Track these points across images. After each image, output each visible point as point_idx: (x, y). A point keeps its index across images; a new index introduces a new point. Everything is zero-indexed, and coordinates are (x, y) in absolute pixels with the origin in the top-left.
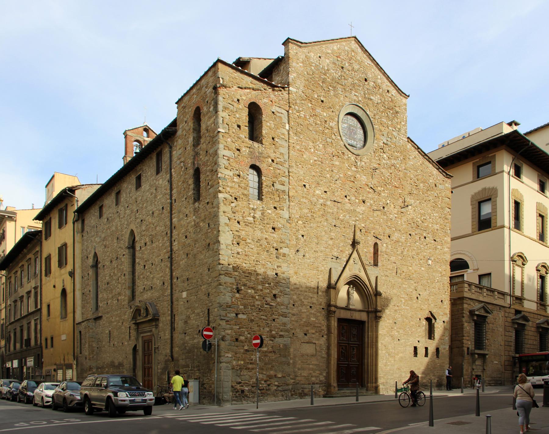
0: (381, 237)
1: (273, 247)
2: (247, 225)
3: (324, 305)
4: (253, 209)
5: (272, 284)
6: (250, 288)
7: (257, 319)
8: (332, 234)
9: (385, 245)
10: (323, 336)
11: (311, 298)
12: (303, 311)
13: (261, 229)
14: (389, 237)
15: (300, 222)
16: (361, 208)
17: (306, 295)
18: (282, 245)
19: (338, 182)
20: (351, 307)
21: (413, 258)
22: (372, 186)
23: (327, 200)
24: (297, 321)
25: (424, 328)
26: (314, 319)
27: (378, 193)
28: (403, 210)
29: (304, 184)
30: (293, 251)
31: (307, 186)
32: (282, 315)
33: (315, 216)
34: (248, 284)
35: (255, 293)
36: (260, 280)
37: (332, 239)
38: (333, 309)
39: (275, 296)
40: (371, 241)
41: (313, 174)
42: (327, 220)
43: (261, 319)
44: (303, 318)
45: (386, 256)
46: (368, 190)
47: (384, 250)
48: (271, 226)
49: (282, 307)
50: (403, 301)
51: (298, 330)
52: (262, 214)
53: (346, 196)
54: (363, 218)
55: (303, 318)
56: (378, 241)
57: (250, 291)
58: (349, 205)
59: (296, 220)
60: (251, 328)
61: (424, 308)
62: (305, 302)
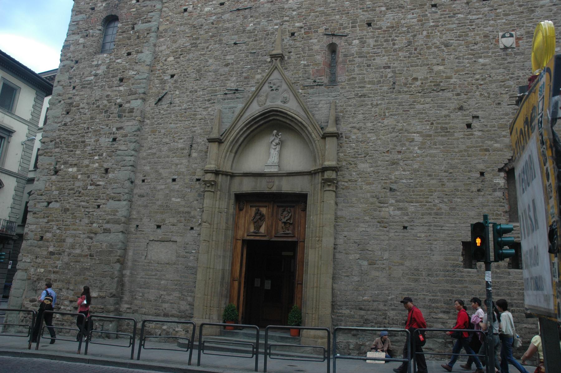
0: (347, 31)
5: (104, 154)
6: (71, 165)
7: (74, 207)
9: (356, 42)
10: (192, 228)
11: (177, 165)
12: (159, 188)
15: (172, 58)
17: (167, 162)
18: (130, 97)
23: (223, 13)
24: (146, 206)
25: (499, 194)
26: (179, 200)
29: (185, 7)
30: (152, 101)
31: (190, 8)
32: (113, 198)
36: (88, 152)
37: (227, 65)
38: (210, 177)
39: (107, 170)
40: (318, 43)
43: (79, 206)
49: (115, 186)
50: (418, 138)
51: (145, 220)
52: (108, 68)
54: (299, 15)
55: (158, 200)
56: (335, 40)
57: (70, 170)
59: (164, 58)
61: (497, 145)
62: (164, 173)
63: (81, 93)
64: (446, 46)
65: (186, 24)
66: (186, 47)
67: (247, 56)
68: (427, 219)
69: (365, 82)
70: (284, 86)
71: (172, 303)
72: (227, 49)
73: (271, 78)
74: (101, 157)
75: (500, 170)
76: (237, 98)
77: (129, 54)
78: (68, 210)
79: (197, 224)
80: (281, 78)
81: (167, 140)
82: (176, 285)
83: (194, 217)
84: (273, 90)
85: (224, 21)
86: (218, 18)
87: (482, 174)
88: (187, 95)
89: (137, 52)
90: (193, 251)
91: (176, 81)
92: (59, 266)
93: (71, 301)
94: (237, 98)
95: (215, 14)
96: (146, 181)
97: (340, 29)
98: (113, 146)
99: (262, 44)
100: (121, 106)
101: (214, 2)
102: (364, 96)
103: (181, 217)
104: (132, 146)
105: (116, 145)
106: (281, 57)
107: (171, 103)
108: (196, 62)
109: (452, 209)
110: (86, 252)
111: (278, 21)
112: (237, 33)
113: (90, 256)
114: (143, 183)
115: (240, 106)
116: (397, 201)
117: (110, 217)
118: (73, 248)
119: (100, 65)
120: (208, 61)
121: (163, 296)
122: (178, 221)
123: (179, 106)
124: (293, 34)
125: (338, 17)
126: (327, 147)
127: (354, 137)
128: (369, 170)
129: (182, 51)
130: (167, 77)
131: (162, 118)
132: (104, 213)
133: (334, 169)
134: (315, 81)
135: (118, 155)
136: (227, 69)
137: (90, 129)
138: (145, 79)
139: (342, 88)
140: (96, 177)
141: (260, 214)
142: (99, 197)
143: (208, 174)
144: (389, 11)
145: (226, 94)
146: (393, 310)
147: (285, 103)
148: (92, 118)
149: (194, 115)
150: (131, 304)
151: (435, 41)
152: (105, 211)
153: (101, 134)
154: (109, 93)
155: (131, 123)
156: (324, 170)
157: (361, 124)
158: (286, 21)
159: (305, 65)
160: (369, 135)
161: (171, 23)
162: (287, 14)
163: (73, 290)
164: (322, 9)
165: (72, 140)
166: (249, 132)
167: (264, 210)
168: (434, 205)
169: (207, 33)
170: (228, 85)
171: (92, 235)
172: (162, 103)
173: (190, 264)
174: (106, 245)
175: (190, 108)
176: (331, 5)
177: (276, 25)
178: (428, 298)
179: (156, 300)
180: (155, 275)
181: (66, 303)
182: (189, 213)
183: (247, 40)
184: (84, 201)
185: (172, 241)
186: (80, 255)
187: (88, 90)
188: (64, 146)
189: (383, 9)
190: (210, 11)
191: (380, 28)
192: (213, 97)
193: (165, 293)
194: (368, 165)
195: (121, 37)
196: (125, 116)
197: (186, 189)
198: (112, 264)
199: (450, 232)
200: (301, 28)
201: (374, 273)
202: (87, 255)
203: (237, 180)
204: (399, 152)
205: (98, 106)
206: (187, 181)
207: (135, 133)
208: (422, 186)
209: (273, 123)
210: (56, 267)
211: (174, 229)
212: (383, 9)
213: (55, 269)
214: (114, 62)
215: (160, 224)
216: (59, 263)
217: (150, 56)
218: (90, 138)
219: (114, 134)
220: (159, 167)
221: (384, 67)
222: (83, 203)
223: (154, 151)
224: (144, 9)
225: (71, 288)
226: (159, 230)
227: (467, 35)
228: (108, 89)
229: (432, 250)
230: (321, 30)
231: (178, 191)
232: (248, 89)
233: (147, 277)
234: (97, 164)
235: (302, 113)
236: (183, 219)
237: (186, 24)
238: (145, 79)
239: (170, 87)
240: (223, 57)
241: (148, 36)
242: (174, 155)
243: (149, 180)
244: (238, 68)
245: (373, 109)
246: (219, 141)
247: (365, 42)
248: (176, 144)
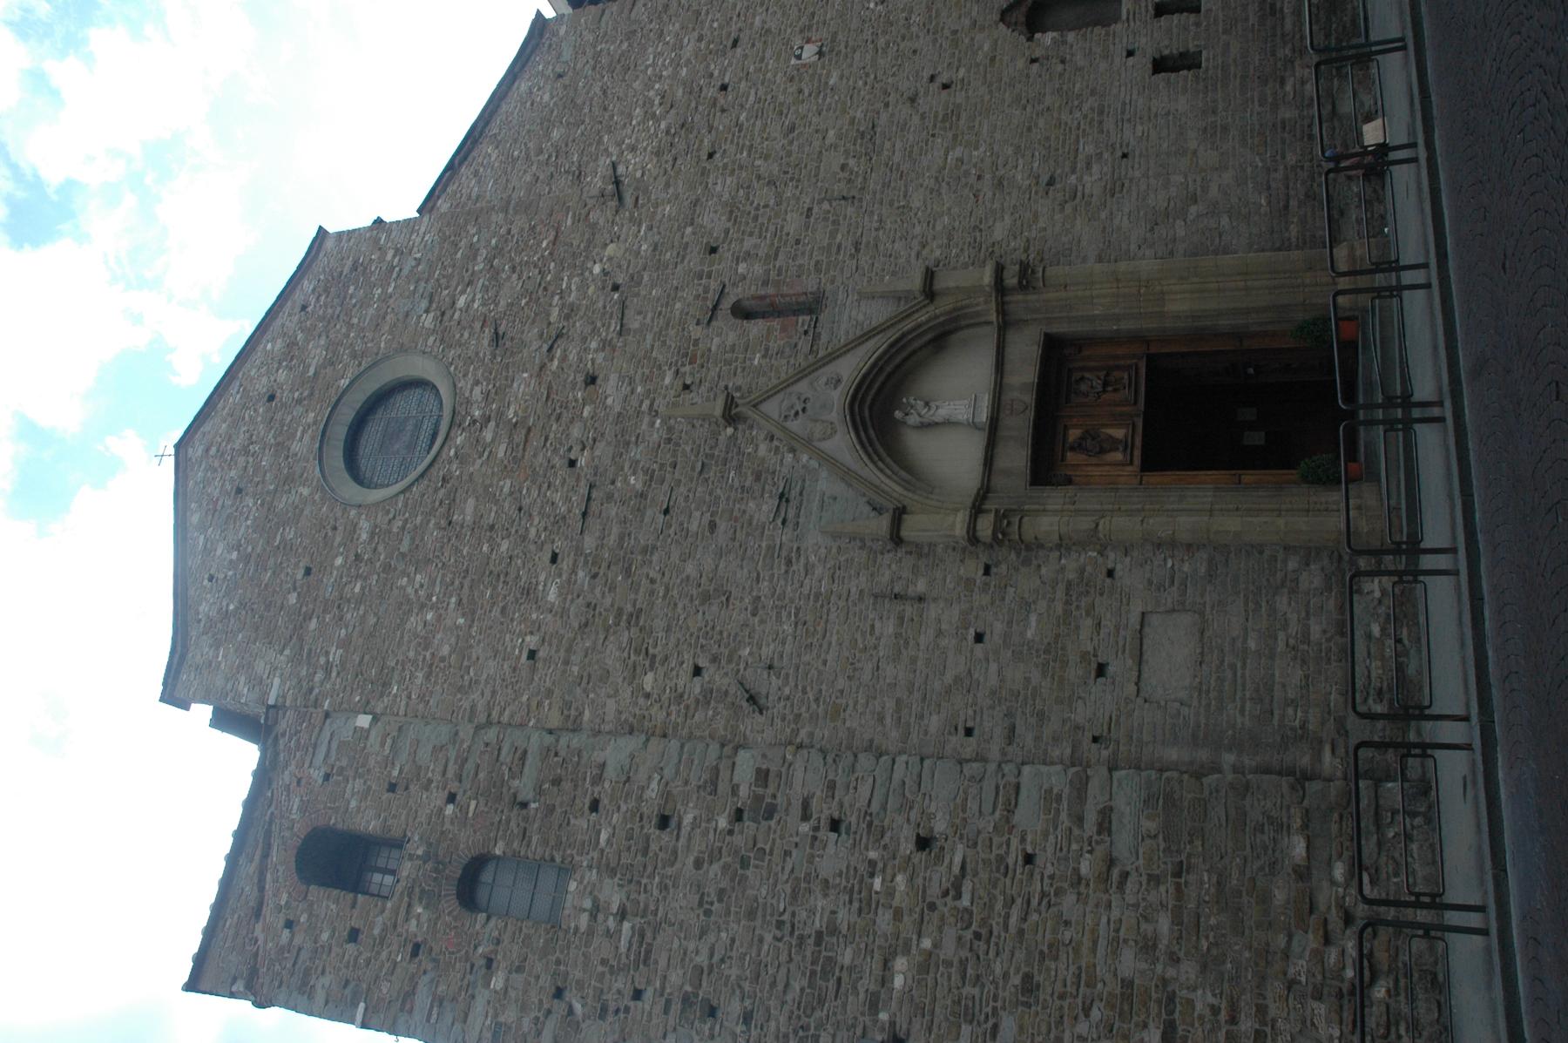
0: (714, 285)
1: (731, 832)
2: (648, 952)
3: (973, 569)
4: (593, 917)
5: (873, 855)
6: (885, 981)
7: (1020, 955)
8: (694, 527)
9: (742, 268)
10: (1110, 573)
11: (940, 633)
12: (993, 680)
13: (664, 888)
14: (713, 250)
15: (648, 681)
16: (612, 392)
18: (723, 787)
19: (526, 502)
20: (983, 417)
21: (792, 129)
22: (545, 347)
23: (579, 550)
24: (1041, 716)
25: (1071, 37)
26: (1033, 618)
27: (567, 317)
28: (629, 200)
29: (525, 655)
30: (752, 724)
31: (532, 641)
32: (1010, 810)
33: (629, 608)
34: (867, 984)
35: (907, 951)
36: (854, 918)
37: (713, 526)
38: (985, 526)
39: (923, 843)
40: (728, 332)
41: (496, 612)
42: (645, 551)
43: (1021, 932)
44: (1027, 680)
45: (781, 257)
46: (556, 362)
47: (758, 269)
48: (653, 832)
49: (973, 805)
50: (958, 152)
51: (1080, 714)
52: (613, 873)
53: (572, 463)
54: (646, 379)
55: (1027, 680)
56: (726, 304)
57: (898, 981)
58: (601, 445)
59: (641, 701)
60: (1062, 997)
61: (986, 47)
63: (662, 963)
64: (792, 129)
65: (569, 650)
66: (631, 640)
67: (706, 480)
68: (1109, 124)
69: (830, 245)
70: (802, 387)
71: (1308, 613)
72: (672, 531)
73: (776, 417)
74: (880, 865)
75: (1030, 39)
76: (801, 494)
77: (595, 806)
78: (1028, 978)
79: (1100, 560)
80: (780, 396)
81: (869, 667)
82: (1258, 604)
83: (1082, 571)
84: (804, 410)
85: (600, 547)
86: (586, 562)
87: (1033, 61)
88: (762, 622)
89: (598, 779)
90: (1169, 564)
91: (715, 659)
92: (1210, 999)
93: (1327, 940)
94: (801, 494)
95: (574, 572)
96: (970, 724)
97: (705, 299)
98: (853, 828)
99: (688, 449)
100: (738, 815)
101: (542, 578)
102: (857, 246)
103: (1078, 607)
104: (865, 761)
105: (853, 819)
106: (730, 403)
107: (770, 667)
108: (679, 609)
109: (1093, 93)
110: (1165, 891)
111: (646, 420)
112: (640, 511)
113: (1178, 874)
114: (976, 732)
115: (825, 483)
116: (1073, 171)
117: (1064, 816)
118: (1155, 946)
119: (596, 902)
120: (688, 577)
121: (1292, 642)
122: (1088, 614)
123: (784, 643)
124: (686, 387)
125: (678, 305)
126: (952, 284)
127: (938, 253)
128: (1008, 219)
129: (638, 652)
130: (697, 686)
131: (804, 688)
132: (1051, 838)
133: (999, 270)
134: (806, 332)
135: (884, 807)
136: (722, 526)
137: (786, 917)
138: (682, 746)
139: (833, 282)
140: (936, 877)
141: (1082, 438)
142: (1001, 859)
143: (979, 527)
144: (698, 221)
145: (784, 522)
146: (1283, 157)
147: (839, 381)
148: (751, 914)
149: (816, 601)
150: (1321, 742)
151: (778, 147)
152: (1046, 834)
153: (808, 874)
154: (691, 859)
155: (799, 775)
156: (999, 287)
157: (915, 243)
158: (652, 405)
159: (764, 356)
160: (939, 228)
161: (549, 693)
162: (635, 403)
163: (1290, 937)
164: (649, 337)
165: (805, 983)
166: (888, 460)
167: (1074, 434)
168: (1085, 117)
169: (612, 589)
170: (763, 519)
171: (1115, 873)
172: (764, 692)
173: (1203, 570)
174: (1148, 818)
175: (798, 610)
176: (648, 320)
177: (652, 424)
178: (1257, 108)
179: (1304, 661)
180: (1233, 667)
181: (1332, 956)
182: (1069, 584)
183: (666, 487)
184: (1007, 916)
185: (1142, 626)
186: (1177, 920)
187: (659, 939)
188: (818, 1014)
189: (689, 230)
190: (560, 588)
191: (727, 232)
192: (784, 553)
193: (1281, 636)
194: (998, 224)
195: (535, 839)
196: (774, 796)
197: (1007, 601)
198: (1207, 793)
199: (1135, 92)
200: (677, 372)
201: (1214, 191)
202: (1178, 886)
203: (998, 482)
204: (979, 178)
205: (721, 893)
206: (986, 599)
207: (829, 759)
208: (1048, 138)
209: (878, 410)
210: (1215, 1010)
211: (1108, 624)
212: (689, 230)
213: (1223, 1016)
214: (602, 851)
215: (1094, 666)
216: (1203, 1000)
217: (622, 742)
218: (812, 912)
219: (816, 829)
220: (937, 685)
221: (808, 217)
222: (1013, 920)
223: (890, 705)
224: (481, 775)
225: (1281, 940)
226: (1111, 669)
227: (781, 104)
228: (678, 865)
229: (1168, 114)
230: (696, 332)
231: (1010, 623)
232: (785, 470)
233: (1239, 694)
234: (899, 878)
235: (870, 344)
236: (1084, 602)
237: (569, 650)
238: (682, 746)
239: (726, 674)
240: (690, 540)
241: (563, 753)
242: (912, 643)
243: (970, 712)
244: (728, 499)
245: (888, 226)
246: (899, 514)
247: (748, 254)
248: (883, 641)
